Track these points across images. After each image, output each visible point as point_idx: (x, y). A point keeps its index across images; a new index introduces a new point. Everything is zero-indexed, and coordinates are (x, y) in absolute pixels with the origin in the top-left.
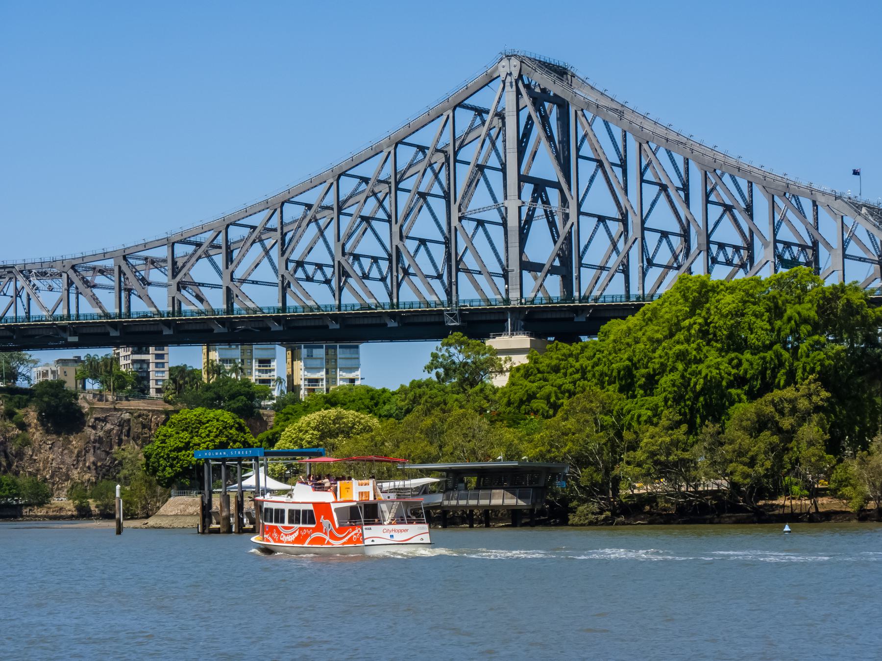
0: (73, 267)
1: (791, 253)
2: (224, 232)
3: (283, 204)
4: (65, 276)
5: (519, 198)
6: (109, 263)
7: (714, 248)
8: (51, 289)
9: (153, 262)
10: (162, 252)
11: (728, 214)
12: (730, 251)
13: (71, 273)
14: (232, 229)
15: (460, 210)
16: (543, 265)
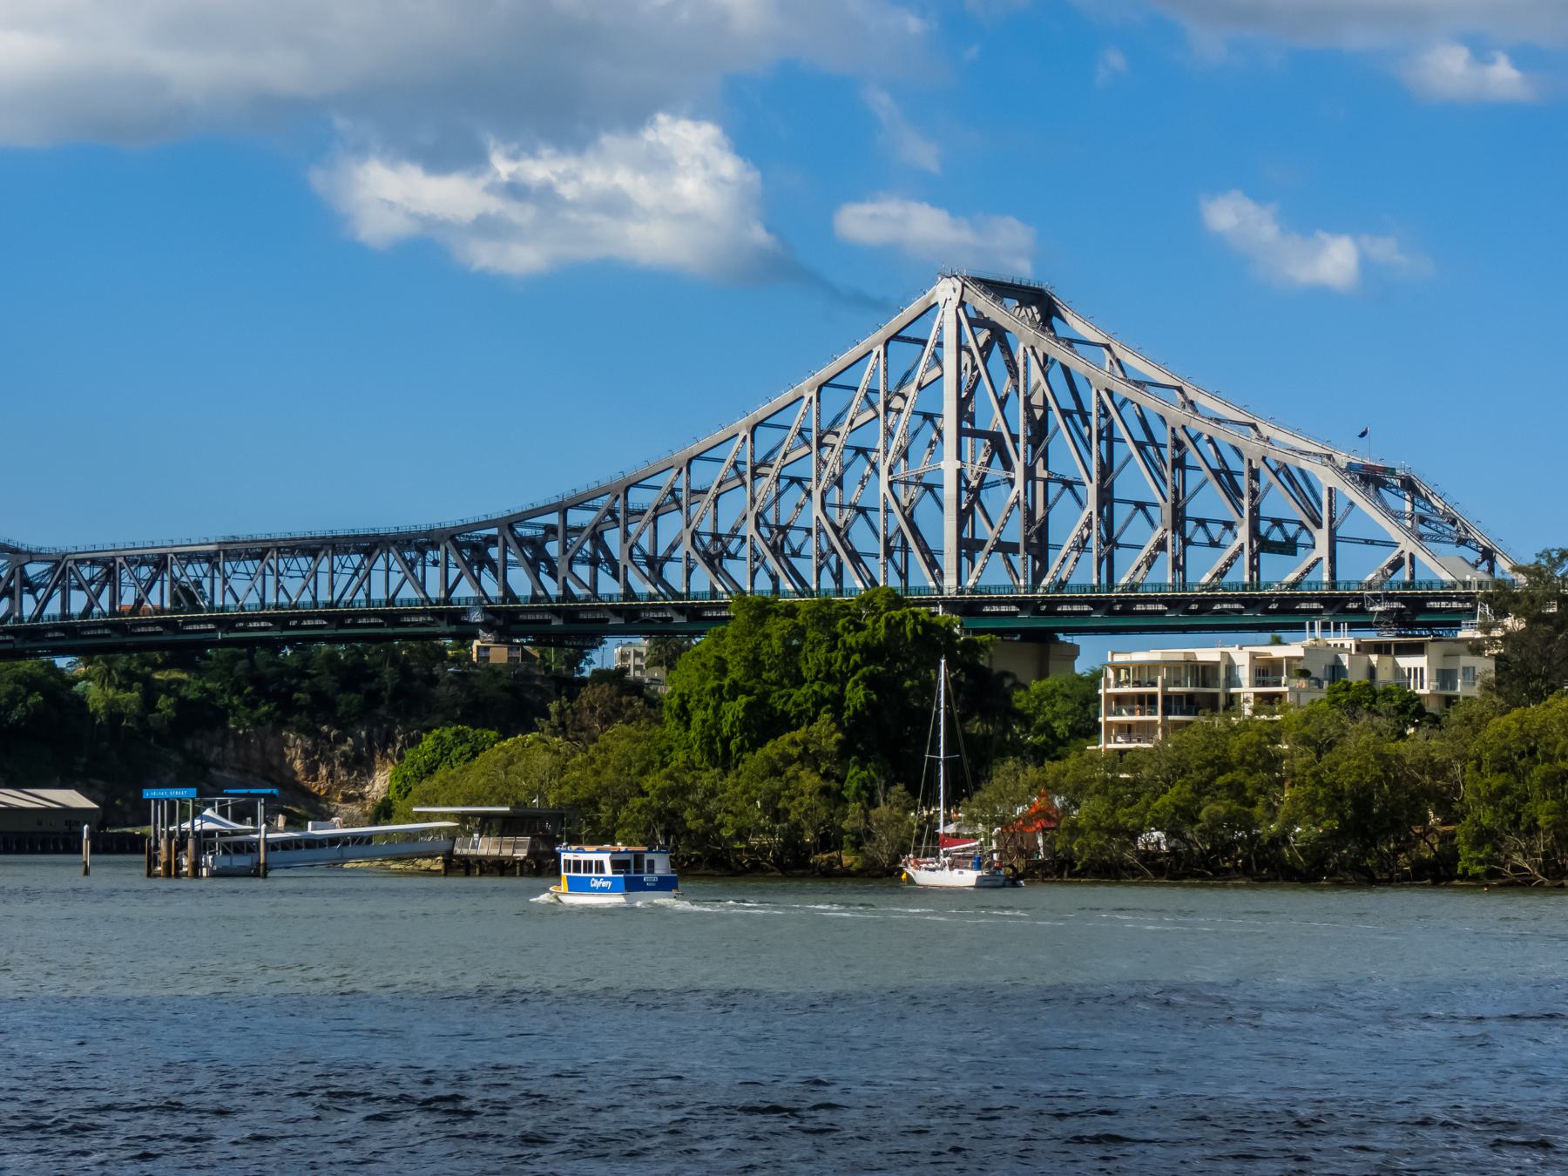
0: (452, 538)
1: (1284, 533)
2: (622, 495)
3: (690, 461)
4: (442, 548)
5: (959, 457)
6: (494, 531)
7: (1190, 525)
8: (435, 563)
9: (551, 530)
10: (553, 519)
11: (1067, 491)
12: (1216, 530)
13: (449, 544)
14: (633, 492)
15: (890, 472)
16: (985, 541)
